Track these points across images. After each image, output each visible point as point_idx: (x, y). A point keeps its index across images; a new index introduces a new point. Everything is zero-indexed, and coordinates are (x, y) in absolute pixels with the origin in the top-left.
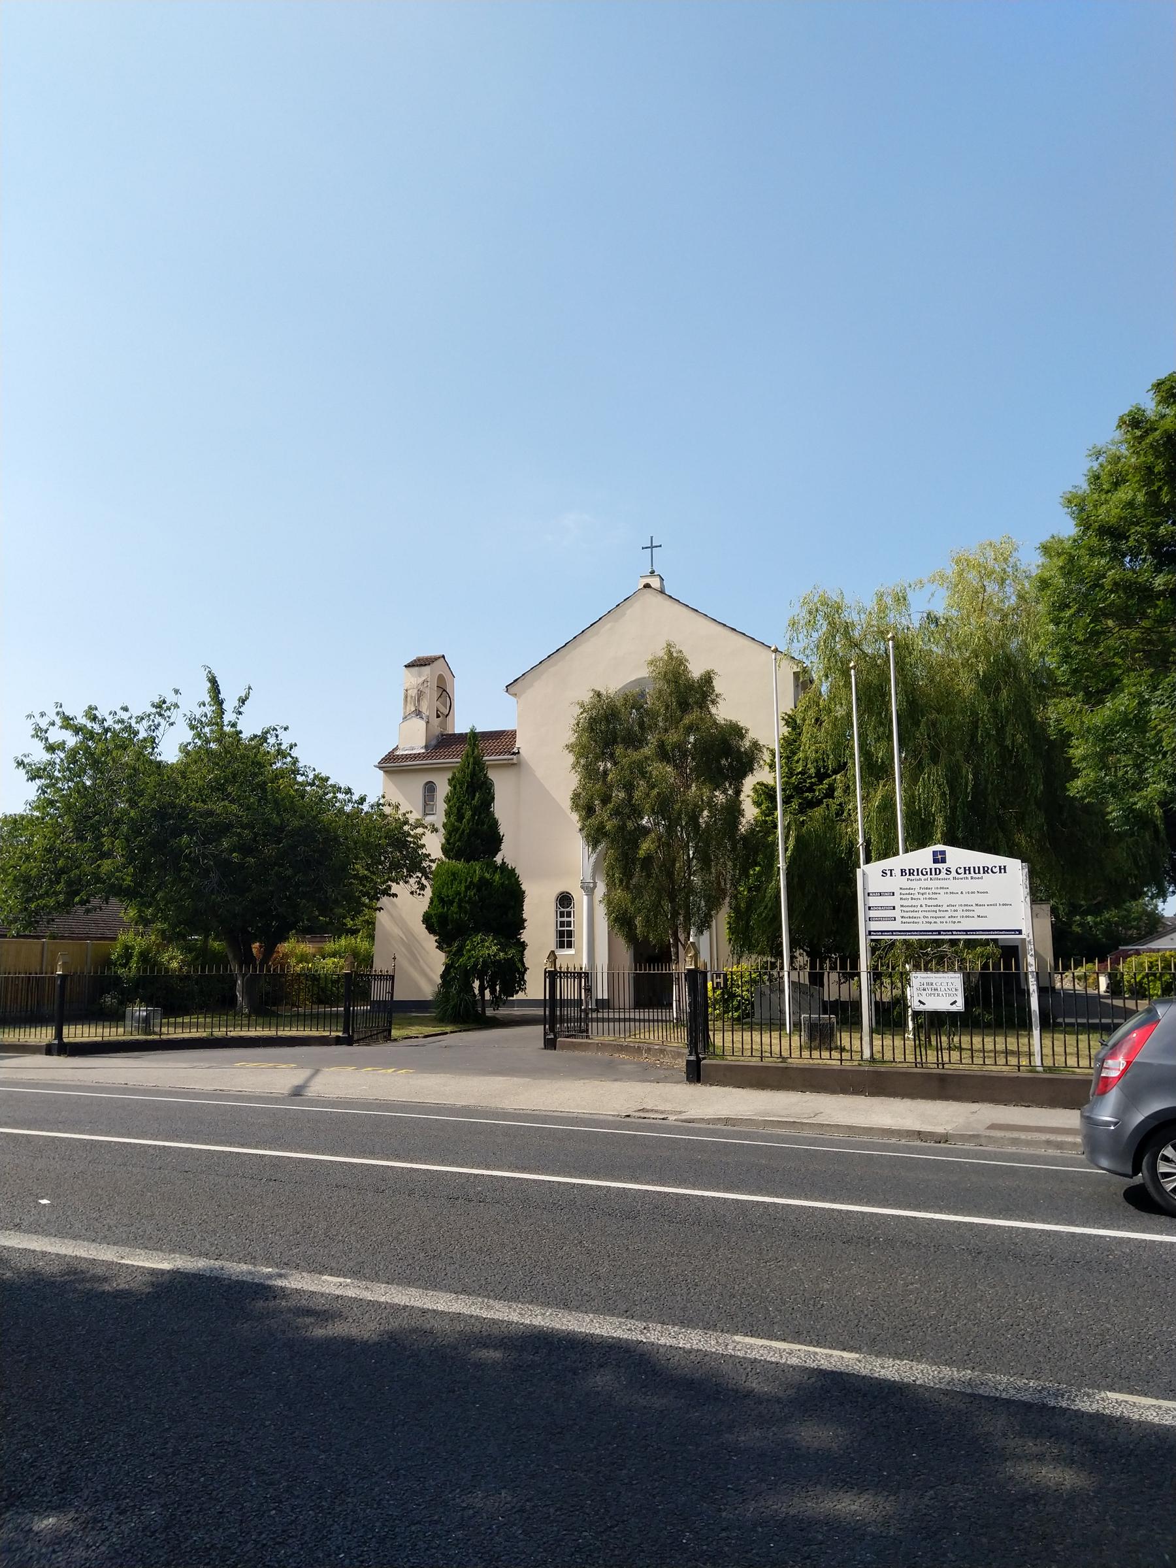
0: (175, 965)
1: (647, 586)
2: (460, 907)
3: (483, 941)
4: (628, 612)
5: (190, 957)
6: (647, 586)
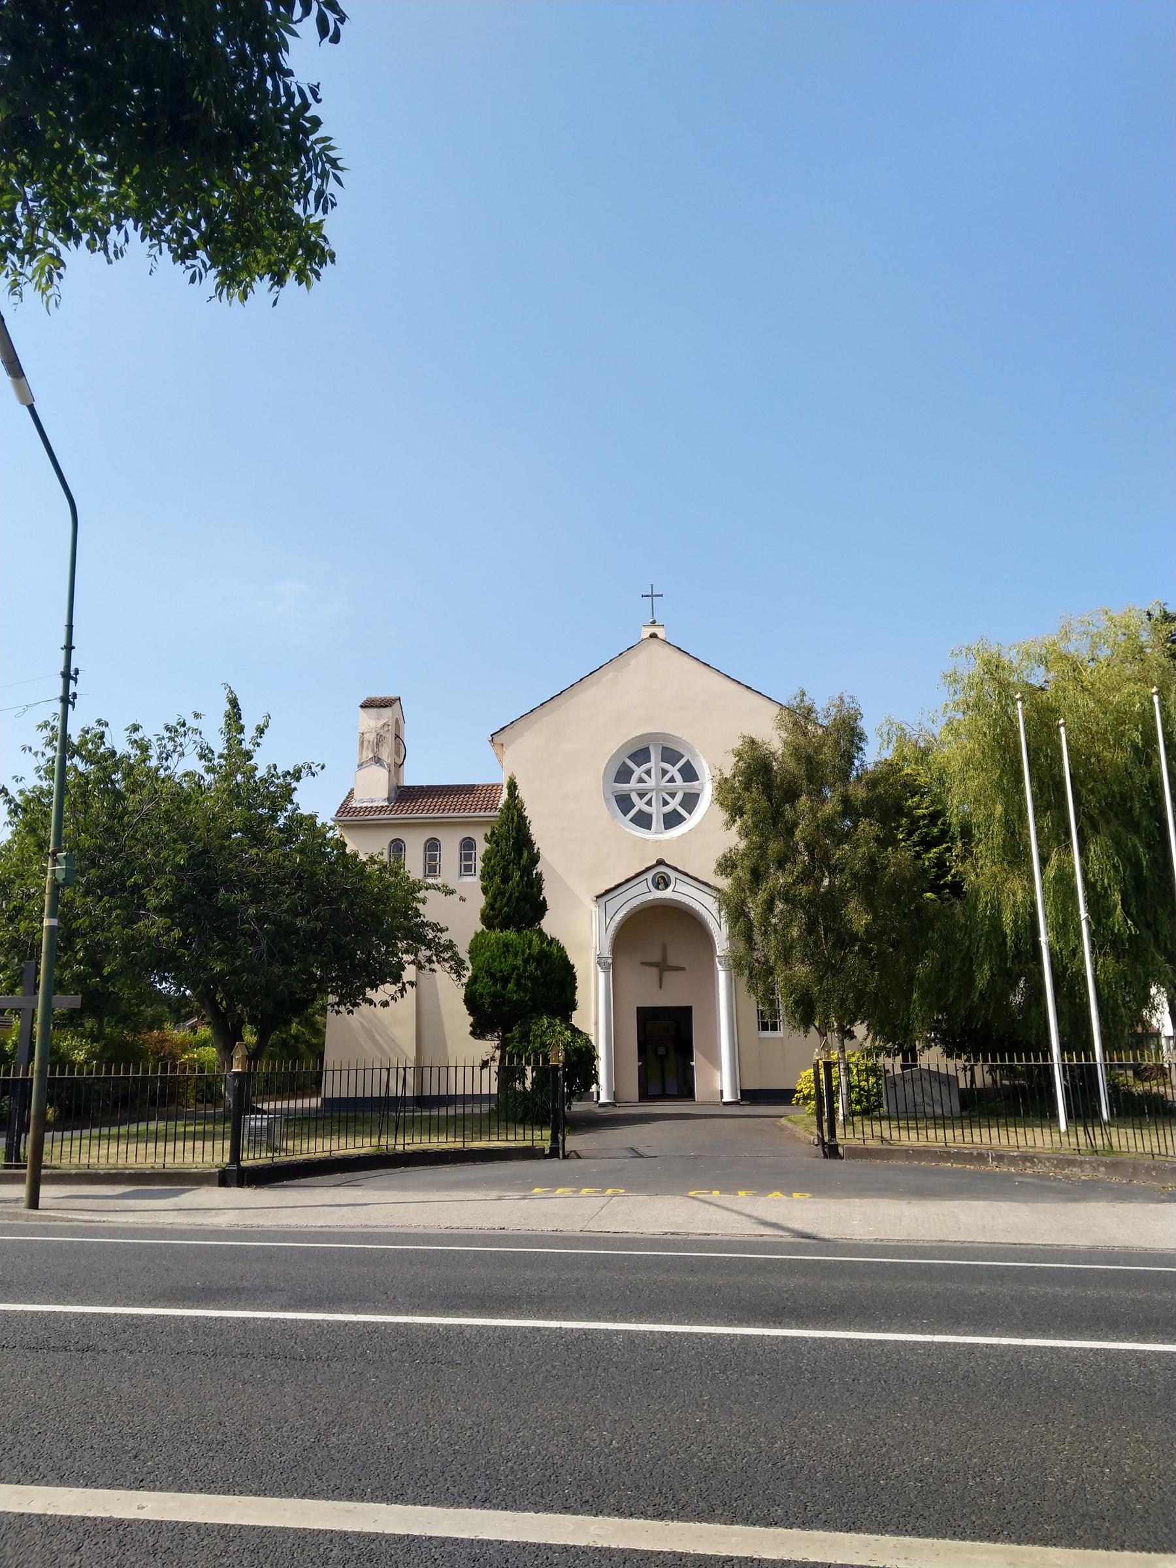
0: (80, 1056)
1: (653, 636)
2: (518, 984)
3: (550, 1025)
4: (633, 662)
5: (97, 1047)
6: (653, 636)
